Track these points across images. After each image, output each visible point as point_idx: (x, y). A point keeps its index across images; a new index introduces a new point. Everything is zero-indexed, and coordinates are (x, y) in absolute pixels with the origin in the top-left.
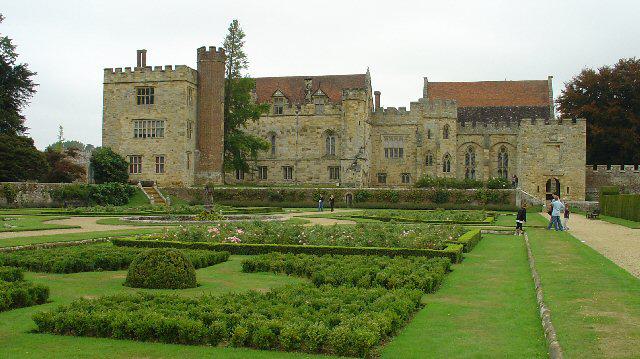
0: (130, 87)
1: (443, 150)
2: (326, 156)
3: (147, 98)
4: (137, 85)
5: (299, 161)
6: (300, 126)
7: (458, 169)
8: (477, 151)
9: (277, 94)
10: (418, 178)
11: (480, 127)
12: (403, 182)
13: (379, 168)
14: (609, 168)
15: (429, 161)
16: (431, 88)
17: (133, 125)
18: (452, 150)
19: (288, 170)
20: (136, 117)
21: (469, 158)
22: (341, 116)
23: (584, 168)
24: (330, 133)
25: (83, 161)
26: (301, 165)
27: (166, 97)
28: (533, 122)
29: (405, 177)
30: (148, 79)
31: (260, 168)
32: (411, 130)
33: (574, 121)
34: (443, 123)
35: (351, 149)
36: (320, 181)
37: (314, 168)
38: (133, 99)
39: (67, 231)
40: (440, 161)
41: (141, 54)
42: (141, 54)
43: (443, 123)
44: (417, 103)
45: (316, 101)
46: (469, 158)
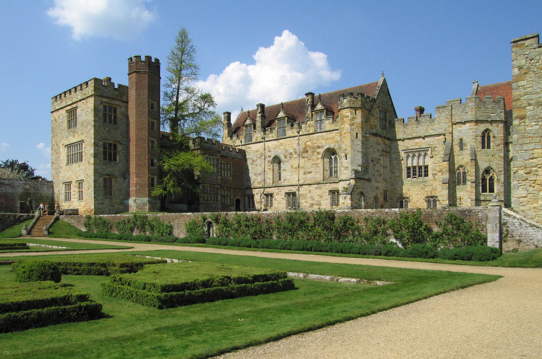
2: (325, 181)
6: (302, 148)
24: (331, 153)
26: (303, 190)
31: (267, 195)
32: (437, 142)
35: (346, 168)
43: (482, 127)
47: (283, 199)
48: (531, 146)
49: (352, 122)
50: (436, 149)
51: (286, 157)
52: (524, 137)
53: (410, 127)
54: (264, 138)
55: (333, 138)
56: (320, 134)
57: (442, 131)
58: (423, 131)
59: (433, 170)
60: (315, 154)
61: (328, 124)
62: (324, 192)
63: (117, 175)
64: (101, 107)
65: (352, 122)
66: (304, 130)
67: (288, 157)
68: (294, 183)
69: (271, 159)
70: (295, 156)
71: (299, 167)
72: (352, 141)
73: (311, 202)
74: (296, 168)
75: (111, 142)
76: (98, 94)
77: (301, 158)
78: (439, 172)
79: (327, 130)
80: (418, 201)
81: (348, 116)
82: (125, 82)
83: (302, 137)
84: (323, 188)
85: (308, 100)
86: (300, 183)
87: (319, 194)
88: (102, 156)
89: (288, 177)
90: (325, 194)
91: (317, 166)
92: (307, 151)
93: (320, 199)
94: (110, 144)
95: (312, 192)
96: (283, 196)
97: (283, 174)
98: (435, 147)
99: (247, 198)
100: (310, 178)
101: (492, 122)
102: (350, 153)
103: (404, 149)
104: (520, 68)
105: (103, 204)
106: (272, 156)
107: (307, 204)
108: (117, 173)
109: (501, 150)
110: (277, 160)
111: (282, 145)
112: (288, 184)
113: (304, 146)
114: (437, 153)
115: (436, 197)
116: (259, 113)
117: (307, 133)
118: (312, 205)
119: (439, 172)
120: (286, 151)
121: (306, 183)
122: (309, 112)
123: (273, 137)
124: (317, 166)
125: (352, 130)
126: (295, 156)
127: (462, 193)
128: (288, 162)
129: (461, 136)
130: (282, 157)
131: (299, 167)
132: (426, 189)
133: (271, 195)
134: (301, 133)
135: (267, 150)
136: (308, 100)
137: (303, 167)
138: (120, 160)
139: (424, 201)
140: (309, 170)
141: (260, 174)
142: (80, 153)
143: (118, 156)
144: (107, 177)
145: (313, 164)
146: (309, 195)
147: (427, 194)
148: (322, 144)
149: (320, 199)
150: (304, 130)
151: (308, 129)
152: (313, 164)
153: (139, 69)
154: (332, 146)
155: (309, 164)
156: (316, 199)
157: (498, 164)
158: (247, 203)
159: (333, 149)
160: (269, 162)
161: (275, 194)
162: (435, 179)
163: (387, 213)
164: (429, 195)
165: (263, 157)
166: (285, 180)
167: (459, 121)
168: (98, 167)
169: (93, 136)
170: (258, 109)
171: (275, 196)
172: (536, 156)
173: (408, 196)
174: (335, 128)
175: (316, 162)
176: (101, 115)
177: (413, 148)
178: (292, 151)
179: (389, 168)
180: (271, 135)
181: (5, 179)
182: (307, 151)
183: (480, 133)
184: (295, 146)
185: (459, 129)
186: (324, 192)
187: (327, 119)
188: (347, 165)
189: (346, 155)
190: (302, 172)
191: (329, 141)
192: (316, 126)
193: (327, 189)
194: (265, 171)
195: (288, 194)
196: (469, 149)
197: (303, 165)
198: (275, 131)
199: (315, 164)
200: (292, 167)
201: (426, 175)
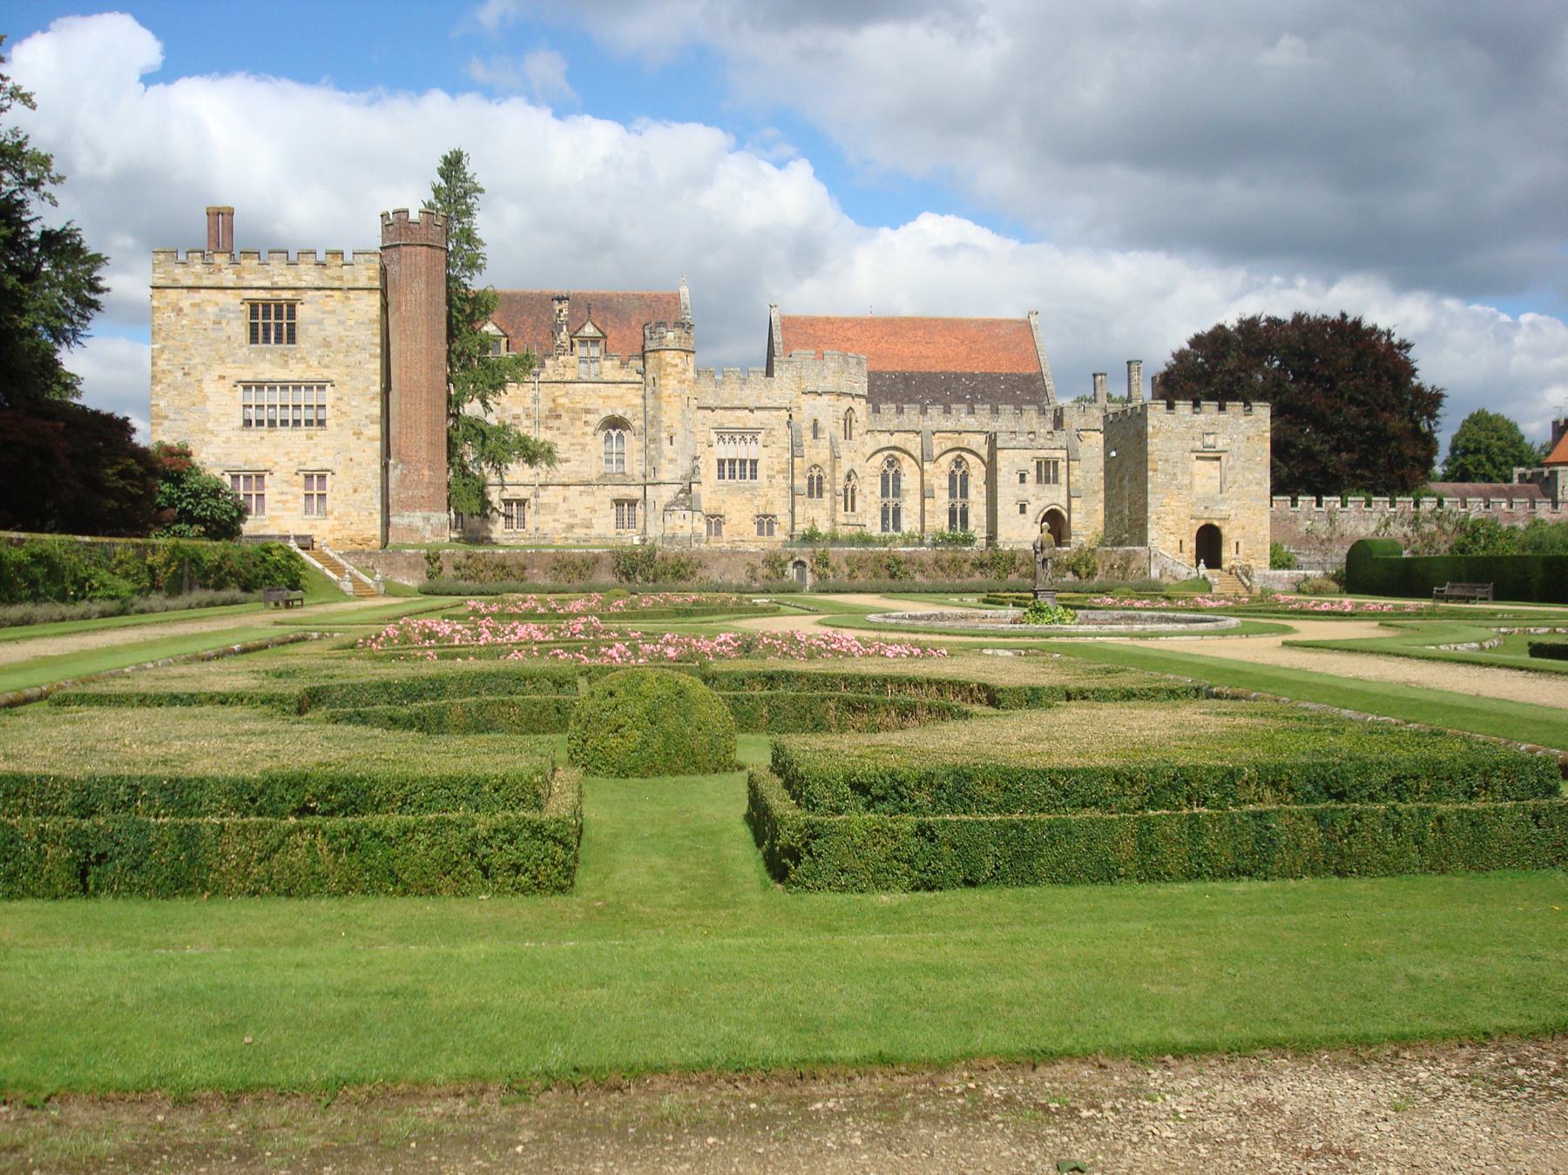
0: (231, 300)
1: (845, 466)
2: (604, 480)
3: (267, 328)
6: (545, 406)
8: (909, 470)
10: (802, 527)
11: (911, 415)
12: (760, 533)
14: (1294, 503)
15: (816, 488)
21: (891, 483)
22: (649, 385)
24: (615, 423)
26: (548, 496)
27: (331, 328)
28: (924, 412)
29: (765, 522)
30: (281, 282)
34: (846, 402)
35: (672, 461)
36: (594, 532)
38: (240, 329)
39: (1070, 640)
40: (840, 488)
45: (580, 351)
46: (891, 483)
53: (728, 389)
55: (621, 397)
56: (590, 385)
57: (786, 403)
59: (769, 468)
60: (579, 424)
66: (550, 371)
78: (778, 472)
79: (606, 379)
84: (598, 493)
85: (561, 311)
91: (583, 449)
103: (715, 425)
107: (558, 525)
113: (551, 405)
118: (571, 527)
119: (778, 472)
121: (555, 481)
122: (564, 336)
124: (583, 449)
127: (815, 511)
129: (816, 415)
132: (756, 502)
145: (572, 445)
150: (550, 371)
152: (572, 445)
154: (619, 413)
162: (771, 485)
164: (762, 512)
167: (812, 389)
173: (722, 513)
174: (625, 379)
175: (581, 440)
177: (732, 425)
182: (559, 417)
183: (842, 414)
184: (528, 402)
185: (812, 402)
188: (674, 456)
191: (613, 403)
199: (579, 444)
201: (753, 477)
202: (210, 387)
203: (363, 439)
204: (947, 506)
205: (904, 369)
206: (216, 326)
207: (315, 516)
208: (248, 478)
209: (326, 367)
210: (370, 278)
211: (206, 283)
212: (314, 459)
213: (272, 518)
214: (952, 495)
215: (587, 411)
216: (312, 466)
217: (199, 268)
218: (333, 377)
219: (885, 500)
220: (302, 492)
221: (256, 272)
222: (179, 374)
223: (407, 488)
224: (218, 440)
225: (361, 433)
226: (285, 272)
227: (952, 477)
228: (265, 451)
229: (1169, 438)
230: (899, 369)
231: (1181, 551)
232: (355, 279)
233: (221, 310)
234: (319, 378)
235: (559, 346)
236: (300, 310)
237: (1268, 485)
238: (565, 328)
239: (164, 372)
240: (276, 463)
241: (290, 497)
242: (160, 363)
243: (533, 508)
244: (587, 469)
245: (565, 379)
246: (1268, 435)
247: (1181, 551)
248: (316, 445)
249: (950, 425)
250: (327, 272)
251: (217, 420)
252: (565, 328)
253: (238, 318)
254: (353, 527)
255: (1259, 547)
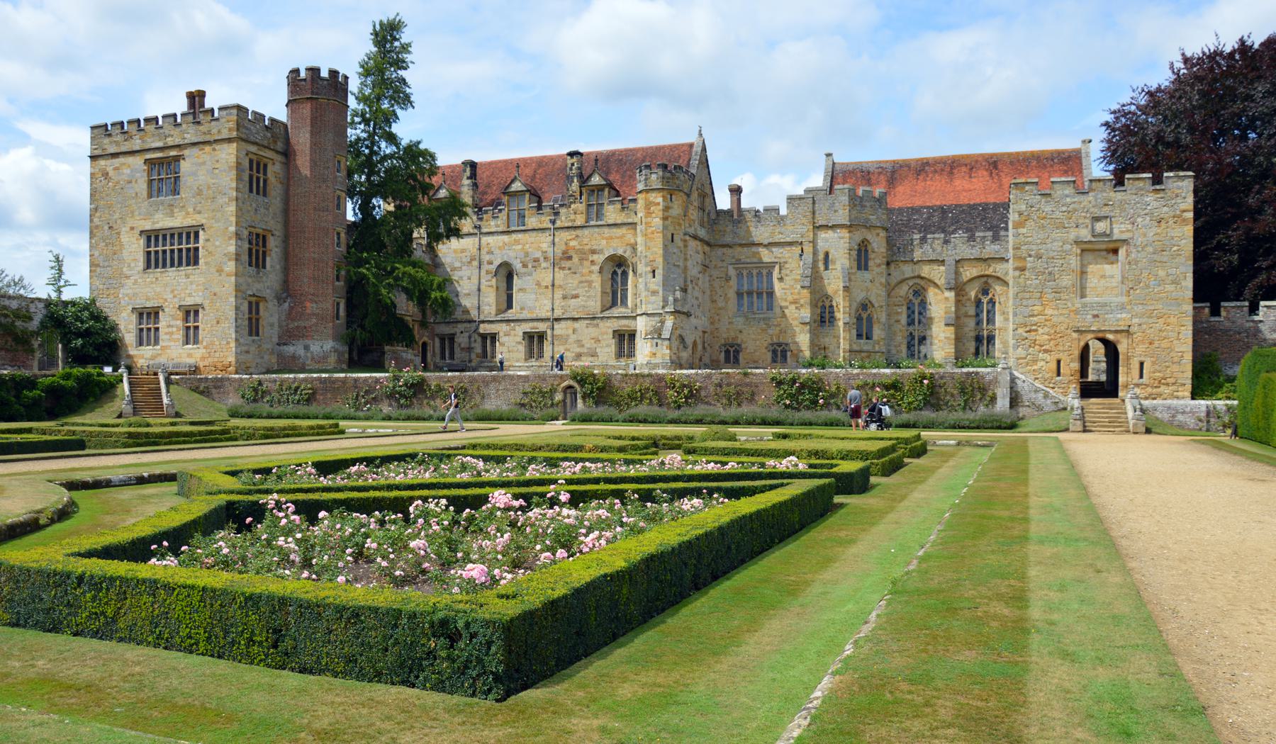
0: (138, 161)
4: (149, 156)
5: (557, 320)
6: (559, 252)
7: (890, 336)
9: (517, 186)
12: (774, 361)
13: (725, 333)
16: (835, 175)
17: (142, 242)
18: (877, 295)
19: (535, 341)
20: (148, 226)
23: (1188, 307)
25: (39, 316)
26: (560, 328)
27: (203, 178)
30: (170, 141)
31: (484, 337)
33: (1157, 180)
37: (585, 332)
38: (142, 186)
41: (196, 98)
42: (196, 98)
43: (858, 236)
44: (800, 198)
47: (520, 343)
48: (1030, 302)
49: (666, 214)
50: (787, 266)
51: (525, 266)
52: (1024, 291)
54: (479, 228)
55: (622, 237)
58: (767, 235)
60: (587, 263)
61: (612, 213)
62: (603, 334)
63: (267, 296)
64: (246, 164)
65: (666, 214)
67: (530, 266)
68: (543, 315)
69: (493, 268)
70: (544, 265)
71: (553, 285)
72: (665, 247)
73: (578, 350)
74: (547, 287)
75: (260, 231)
76: (243, 136)
77: (556, 270)
78: (791, 303)
79: (611, 222)
80: (755, 351)
81: (658, 204)
82: (282, 115)
83: (560, 231)
85: (573, 164)
86: (556, 316)
87: (593, 335)
88: (245, 258)
89: (530, 304)
90: (605, 337)
91: (590, 286)
92: (570, 258)
93: (595, 345)
94: (258, 235)
95: (580, 331)
96: (520, 339)
97: (517, 297)
98: (786, 263)
99: (437, 341)
100: (574, 308)
101: (870, 227)
102: (661, 267)
104: (1020, 214)
105: (247, 352)
106: (497, 263)
108: (268, 293)
109: (882, 273)
110: (507, 274)
111: (517, 242)
112: (529, 316)
113: (563, 247)
114: (788, 272)
115: (787, 344)
116: (468, 178)
117: (570, 224)
120: (527, 254)
123: (497, 226)
124: (590, 286)
125: (665, 227)
126: (544, 265)
127: (827, 339)
128: (530, 274)
130: (517, 266)
131: (553, 285)
133: (494, 337)
134: (558, 224)
135: (484, 252)
136: (573, 164)
137: (560, 286)
138: (272, 266)
139: (764, 351)
140: (574, 292)
141: (469, 294)
142: (188, 250)
143: (268, 259)
144: (253, 299)
145: (581, 282)
146: (573, 338)
147: (772, 339)
148: (601, 247)
149: (595, 345)
151: (572, 217)
152: (581, 282)
153: (317, 94)
154: (620, 252)
155: (573, 282)
156: (588, 345)
157: (878, 295)
158: (438, 350)
159: (621, 257)
160: (488, 272)
161: (501, 334)
163: (875, 374)
164: (775, 340)
165: (475, 263)
166: (522, 309)
167: (824, 223)
168: (241, 280)
169: (233, 219)
170: (465, 171)
171: (503, 339)
172: (1036, 313)
173: (739, 342)
175: (588, 278)
176: (246, 178)
177: (748, 260)
178: (538, 255)
179: (708, 293)
180: (491, 224)
181: (10, 297)
182: (570, 258)
184: (545, 246)
185: (823, 235)
186: (603, 334)
187: (611, 202)
188: (656, 288)
189: (654, 272)
190: (559, 294)
191: (615, 243)
192: (588, 213)
193: (609, 327)
194: (479, 290)
195: (529, 337)
196: (839, 268)
197: (562, 283)
198: (503, 216)
199: (586, 282)
200: (538, 284)
202: (125, 238)
203: (224, 275)
204: (973, 334)
205: (944, 203)
206: (130, 185)
207: (190, 346)
208: (149, 314)
209: (199, 213)
210: (230, 130)
211: (124, 149)
212: (190, 295)
213: (163, 348)
214: (978, 323)
215: (593, 252)
216: (189, 301)
217: (119, 138)
218: (204, 221)
219: (911, 328)
220: (180, 323)
221: (153, 135)
222: (106, 227)
223: (293, 320)
224: (129, 282)
225: (222, 271)
226: (172, 133)
227: (978, 303)
228: (158, 289)
229: (1043, 227)
230: (938, 203)
231: (1059, 374)
232: (219, 132)
233: (132, 171)
234: (194, 223)
235: (572, 196)
236: (185, 166)
237: (1189, 283)
238: (575, 180)
239: (97, 227)
240: (166, 300)
241: (174, 329)
242: (96, 220)
243: (549, 339)
244: (593, 304)
245: (575, 224)
246: (1191, 215)
247: (1059, 374)
248: (191, 283)
249: (975, 252)
250: (201, 128)
251: (129, 266)
252: (575, 180)
253: (142, 177)
254: (217, 355)
255: (1175, 368)
